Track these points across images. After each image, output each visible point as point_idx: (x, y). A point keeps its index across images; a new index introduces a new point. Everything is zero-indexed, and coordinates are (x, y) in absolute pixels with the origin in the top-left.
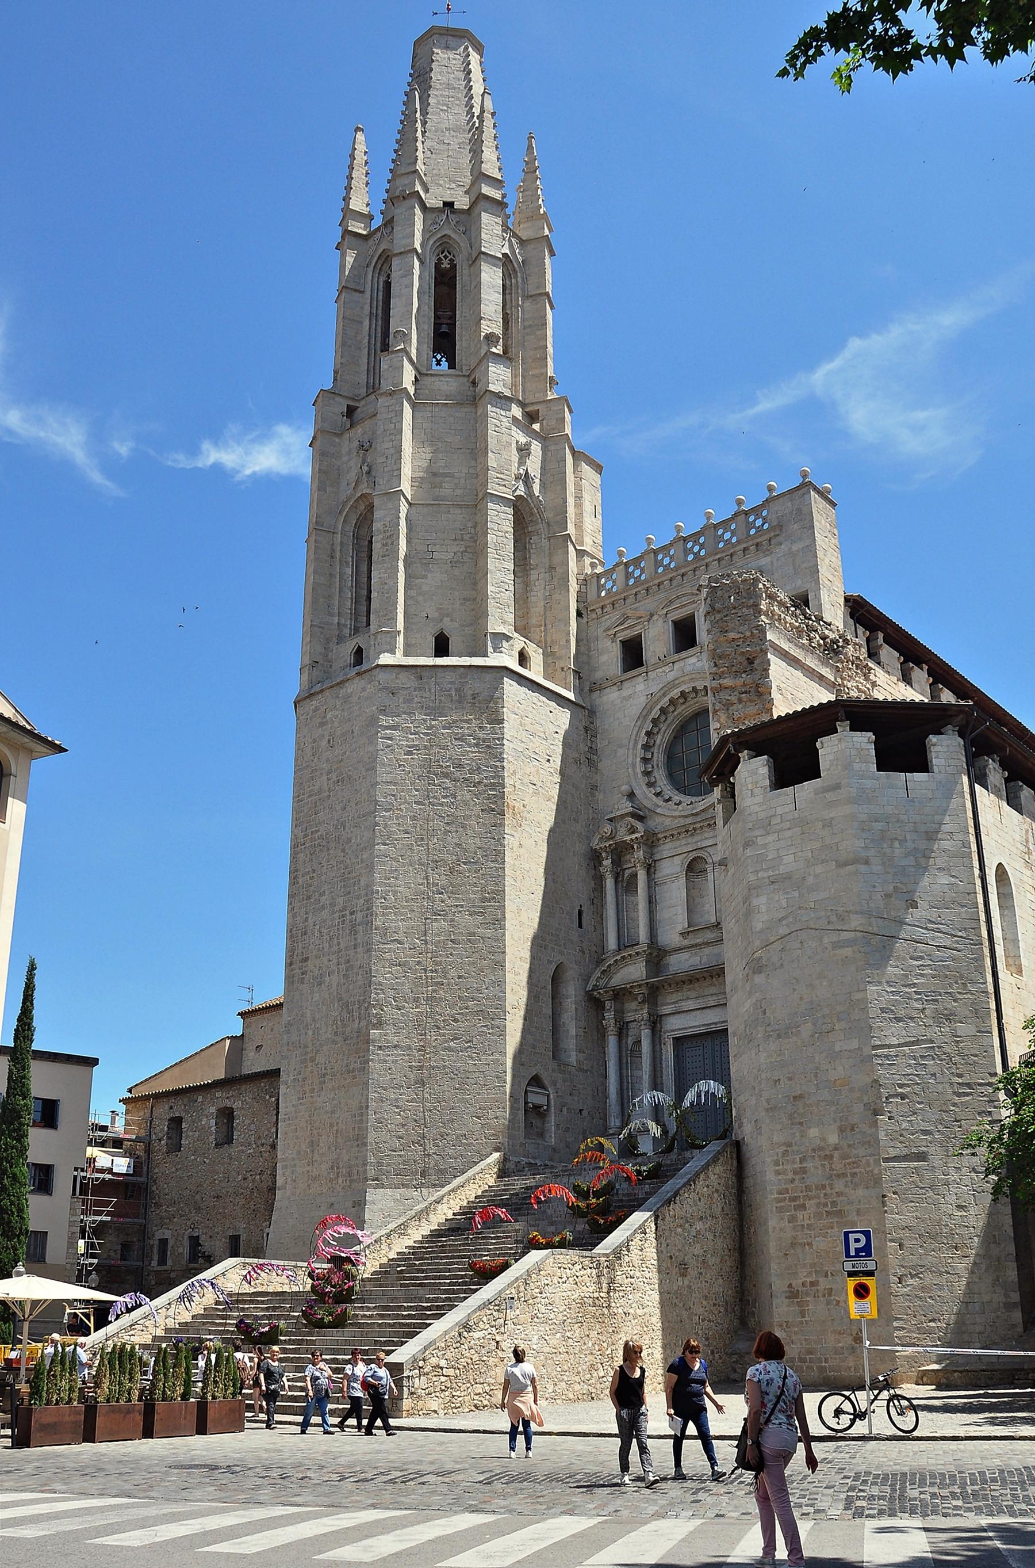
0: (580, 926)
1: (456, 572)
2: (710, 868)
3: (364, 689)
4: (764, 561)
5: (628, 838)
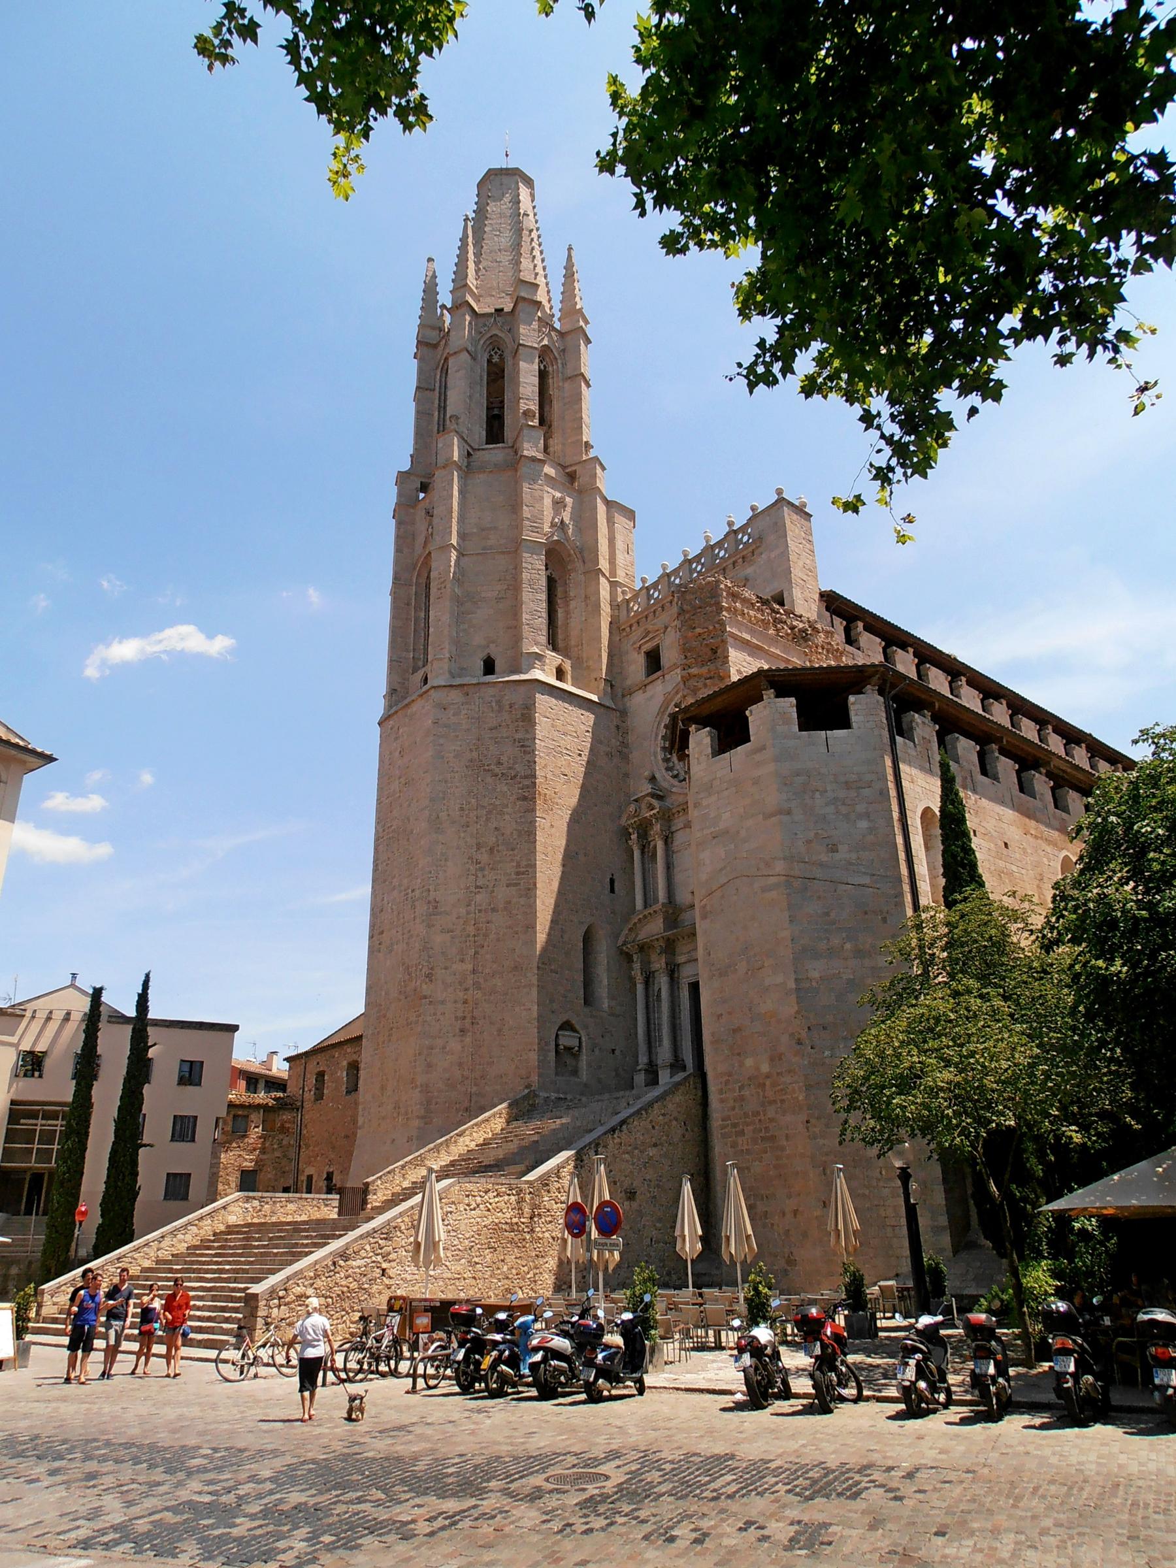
0: (612, 891)
3: (423, 707)
4: (749, 571)
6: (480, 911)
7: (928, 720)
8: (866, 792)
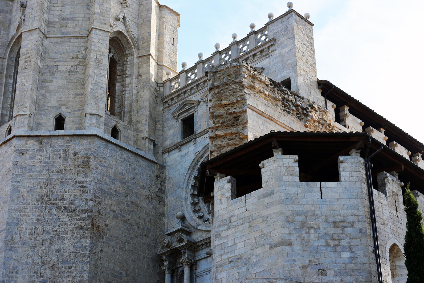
1: (72, 77)
3: (6, 152)
7: (396, 179)
8: (349, 230)
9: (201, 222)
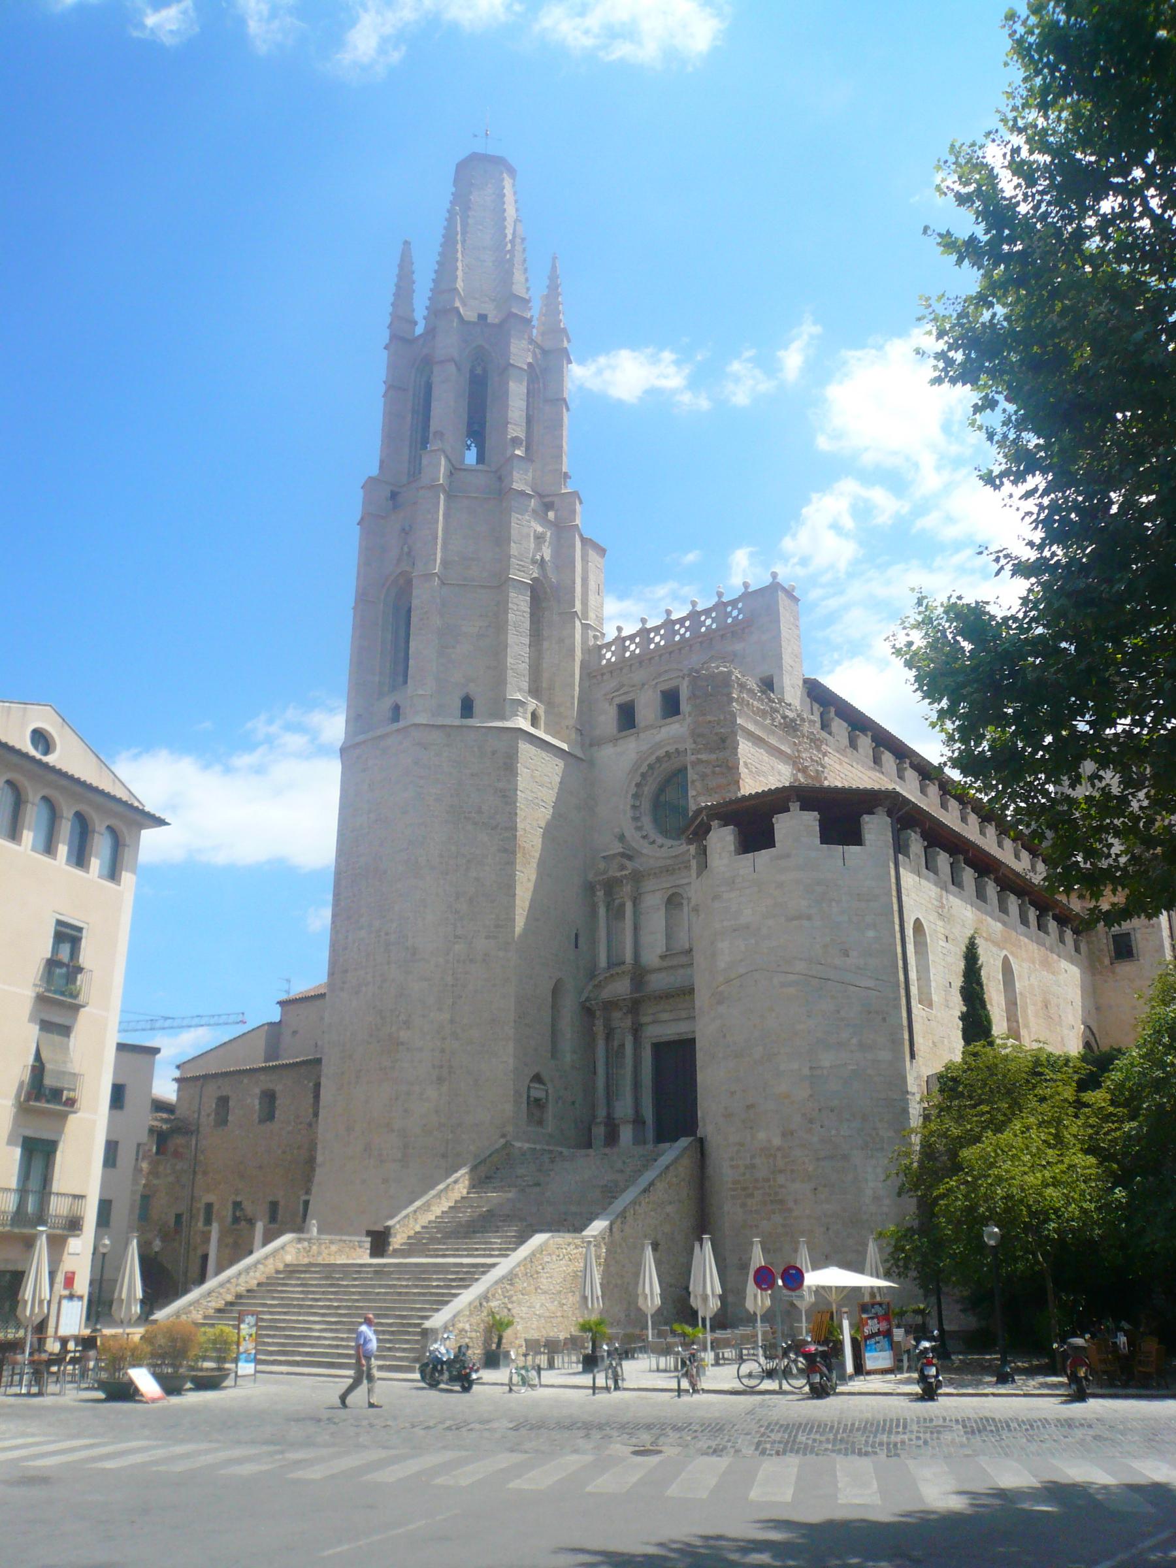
0: (576, 947)
2: (685, 902)
4: (738, 647)
5: (618, 874)
6: (458, 961)
7: (918, 837)
9: (645, 843)
